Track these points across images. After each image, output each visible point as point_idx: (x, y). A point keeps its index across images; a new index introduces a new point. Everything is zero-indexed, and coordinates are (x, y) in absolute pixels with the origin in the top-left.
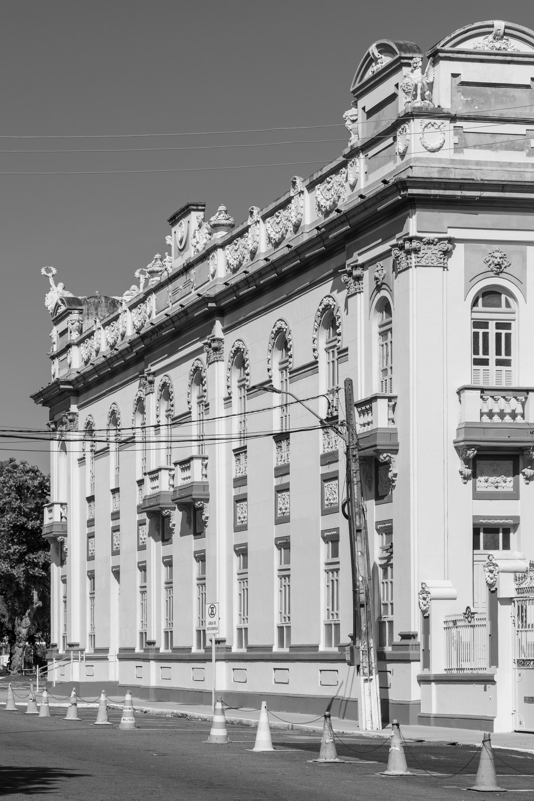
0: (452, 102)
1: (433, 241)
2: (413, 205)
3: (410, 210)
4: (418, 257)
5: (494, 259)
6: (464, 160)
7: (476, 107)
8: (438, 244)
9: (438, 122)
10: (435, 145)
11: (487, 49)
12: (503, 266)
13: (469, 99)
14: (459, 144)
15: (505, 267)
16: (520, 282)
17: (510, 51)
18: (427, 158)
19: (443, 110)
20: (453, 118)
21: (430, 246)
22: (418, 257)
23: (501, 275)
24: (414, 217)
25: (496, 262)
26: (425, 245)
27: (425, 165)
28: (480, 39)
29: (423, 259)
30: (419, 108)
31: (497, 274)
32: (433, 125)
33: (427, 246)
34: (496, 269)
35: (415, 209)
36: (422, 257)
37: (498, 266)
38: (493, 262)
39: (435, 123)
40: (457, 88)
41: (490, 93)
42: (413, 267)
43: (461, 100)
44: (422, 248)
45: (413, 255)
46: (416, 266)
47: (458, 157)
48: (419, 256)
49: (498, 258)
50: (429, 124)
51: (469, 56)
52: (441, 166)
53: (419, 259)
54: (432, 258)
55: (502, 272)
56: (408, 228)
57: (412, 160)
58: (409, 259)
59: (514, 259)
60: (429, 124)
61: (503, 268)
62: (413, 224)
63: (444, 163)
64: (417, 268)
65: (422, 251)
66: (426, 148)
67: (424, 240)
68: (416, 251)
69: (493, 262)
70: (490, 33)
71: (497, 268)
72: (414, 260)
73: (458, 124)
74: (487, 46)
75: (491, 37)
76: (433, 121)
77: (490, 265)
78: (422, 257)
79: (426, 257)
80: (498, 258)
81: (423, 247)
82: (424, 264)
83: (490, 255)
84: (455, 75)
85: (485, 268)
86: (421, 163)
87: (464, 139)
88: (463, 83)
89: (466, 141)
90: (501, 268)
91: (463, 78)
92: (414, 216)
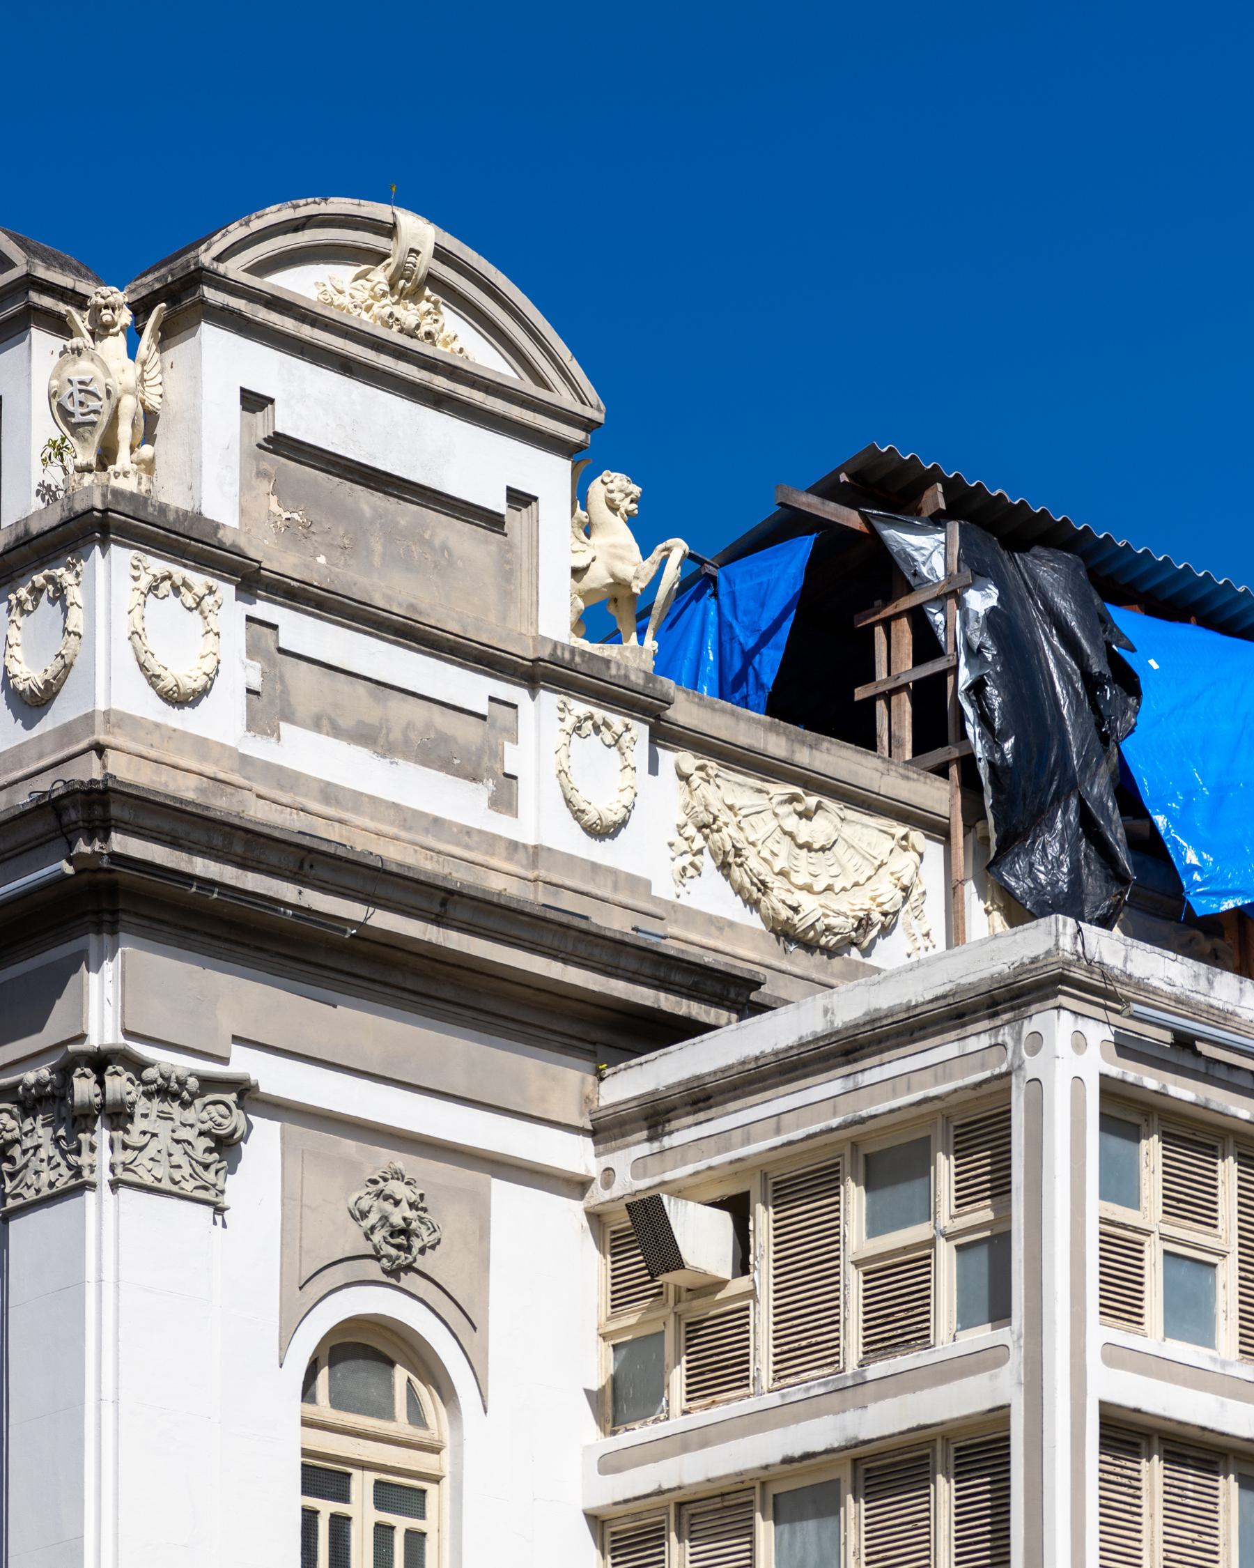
0: (243, 512)
1: (182, 1083)
2: (107, 917)
3: (92, 937)
4: (125, 1147)
5: (388, 1206)
6: (280, 769)
7: (322, 560)
8: (198, 1103)
9: (199, 581)
10: (183, 671)
11: (367, 321)
12: (417, 1244)
13: (296, 516)
14: (264, 698)
15: (422, 1251)
16: (467, 1320)
17: (439, 351)
18: (157, 725)
19: (221, 534)
20: (251, 580)
21: (165, 1107)
22: (125, 1147)
23: (408, 1280)
24: (110, 968)
25: (397, 1220)
26: (149, 1095)
27: (153, 754)
28: (343, 274)
29: (143, 1158)
30: (133, 497)
31: (394, 1273)
32: (176, 590)
33: (156, 1105)
34: (393, 1252)
35: (114, 932)
36: (141, 1149)
37: (401, 1240)
38: (385, 1218)
39: (185, 584)
40: (258, 459)
41: (368, 512)
42: (106, 1188)
43: (270, 514)
44: (139, 1110)
45: (103, 1135)
46: (115, 1185)
47: (259, 748)
48: (127, 1138)
49: (404, 1205)
50: (164, 579)
51: (307, 332)
52: (210, 770)
53: (130, 1155)
54: (176, 1160)
55: (409, 1268)
56: (80, 1011)
57: (99, 720)
58: (85, 1149)
59: (449, 1219)
60: (164, 579)
61: (415, 1251)
62: (105, 998)
63: (216, 762)
64: (124, 1192)
65: (139, 1124)
66: (153, 679)
67: (149, 1074)
68: (119, 1116)
69: (385, 1218)
70: (379, 257)
71: (398, 1247)
72: (105, 1156)
73: (263, 609)
74: (368, 309)
75: (380, 276)
76: (179, 572)
77: (373, 1228)
78: (141, 1149)
79: (151, 1151)
80: (404, 1205)
81: (142, 1105)
82: (148, 1180)
83: (373, 1188)
84: (253, 402)
85: (352, 1240)
86: (134, 739)
87: (282, 679)
88: (280, 444)
89: (285, 691)
90: (408, 1249)
91: (286, 421)
92: (108, 966)
